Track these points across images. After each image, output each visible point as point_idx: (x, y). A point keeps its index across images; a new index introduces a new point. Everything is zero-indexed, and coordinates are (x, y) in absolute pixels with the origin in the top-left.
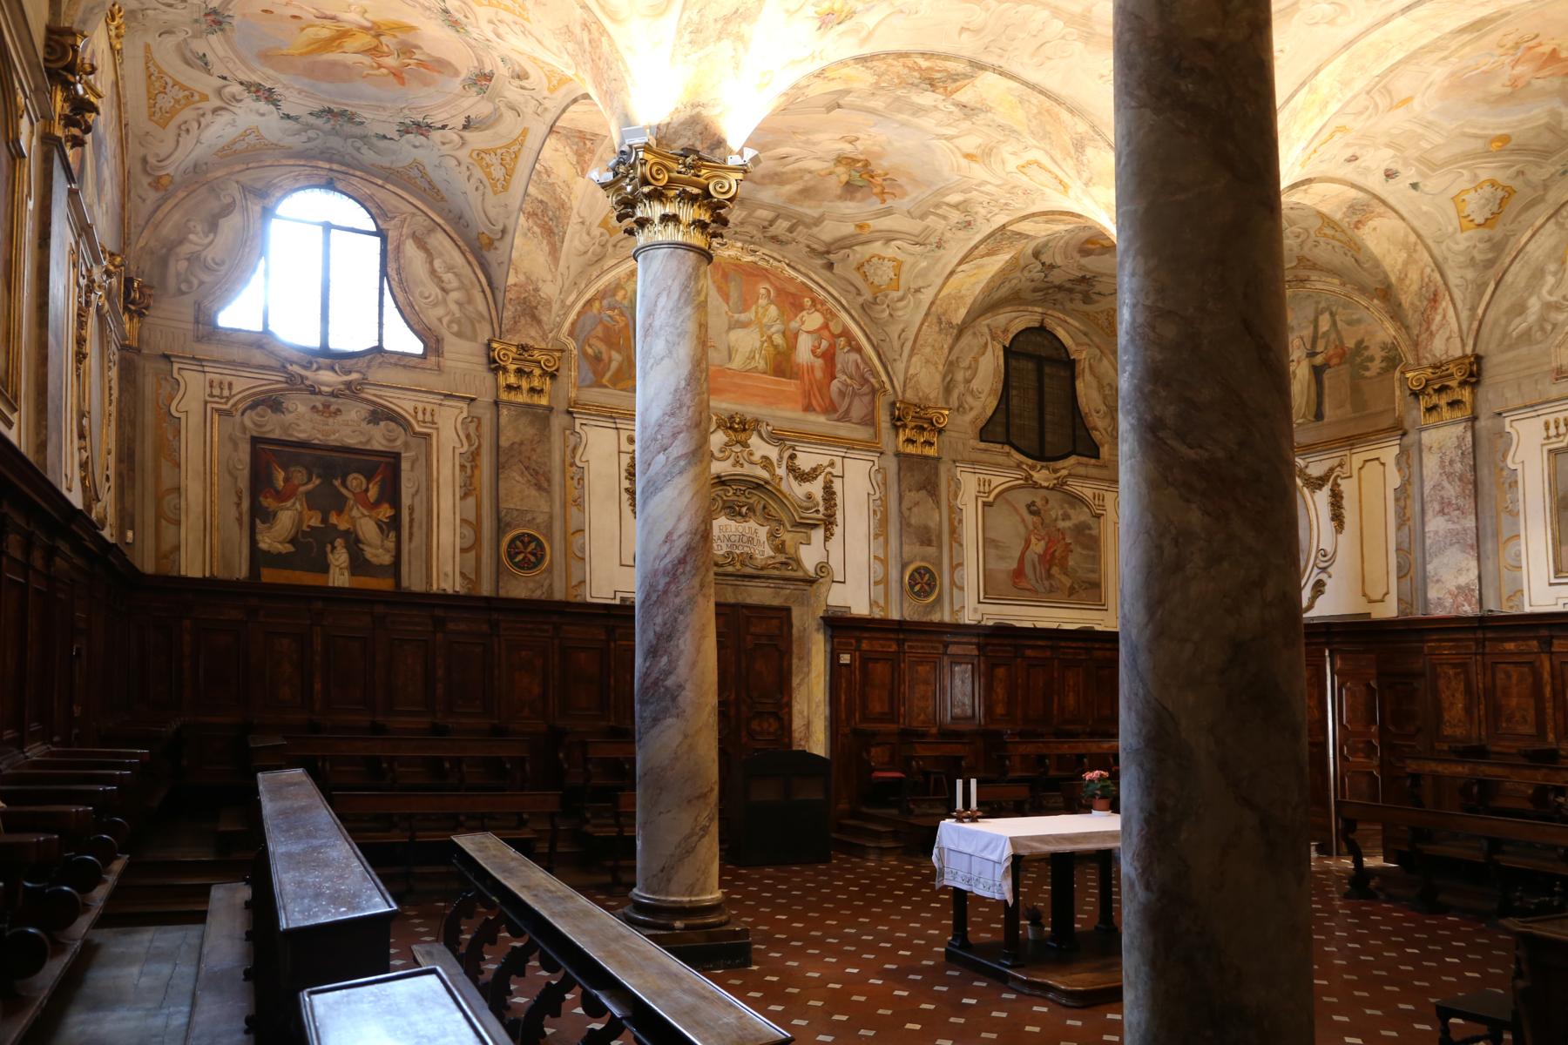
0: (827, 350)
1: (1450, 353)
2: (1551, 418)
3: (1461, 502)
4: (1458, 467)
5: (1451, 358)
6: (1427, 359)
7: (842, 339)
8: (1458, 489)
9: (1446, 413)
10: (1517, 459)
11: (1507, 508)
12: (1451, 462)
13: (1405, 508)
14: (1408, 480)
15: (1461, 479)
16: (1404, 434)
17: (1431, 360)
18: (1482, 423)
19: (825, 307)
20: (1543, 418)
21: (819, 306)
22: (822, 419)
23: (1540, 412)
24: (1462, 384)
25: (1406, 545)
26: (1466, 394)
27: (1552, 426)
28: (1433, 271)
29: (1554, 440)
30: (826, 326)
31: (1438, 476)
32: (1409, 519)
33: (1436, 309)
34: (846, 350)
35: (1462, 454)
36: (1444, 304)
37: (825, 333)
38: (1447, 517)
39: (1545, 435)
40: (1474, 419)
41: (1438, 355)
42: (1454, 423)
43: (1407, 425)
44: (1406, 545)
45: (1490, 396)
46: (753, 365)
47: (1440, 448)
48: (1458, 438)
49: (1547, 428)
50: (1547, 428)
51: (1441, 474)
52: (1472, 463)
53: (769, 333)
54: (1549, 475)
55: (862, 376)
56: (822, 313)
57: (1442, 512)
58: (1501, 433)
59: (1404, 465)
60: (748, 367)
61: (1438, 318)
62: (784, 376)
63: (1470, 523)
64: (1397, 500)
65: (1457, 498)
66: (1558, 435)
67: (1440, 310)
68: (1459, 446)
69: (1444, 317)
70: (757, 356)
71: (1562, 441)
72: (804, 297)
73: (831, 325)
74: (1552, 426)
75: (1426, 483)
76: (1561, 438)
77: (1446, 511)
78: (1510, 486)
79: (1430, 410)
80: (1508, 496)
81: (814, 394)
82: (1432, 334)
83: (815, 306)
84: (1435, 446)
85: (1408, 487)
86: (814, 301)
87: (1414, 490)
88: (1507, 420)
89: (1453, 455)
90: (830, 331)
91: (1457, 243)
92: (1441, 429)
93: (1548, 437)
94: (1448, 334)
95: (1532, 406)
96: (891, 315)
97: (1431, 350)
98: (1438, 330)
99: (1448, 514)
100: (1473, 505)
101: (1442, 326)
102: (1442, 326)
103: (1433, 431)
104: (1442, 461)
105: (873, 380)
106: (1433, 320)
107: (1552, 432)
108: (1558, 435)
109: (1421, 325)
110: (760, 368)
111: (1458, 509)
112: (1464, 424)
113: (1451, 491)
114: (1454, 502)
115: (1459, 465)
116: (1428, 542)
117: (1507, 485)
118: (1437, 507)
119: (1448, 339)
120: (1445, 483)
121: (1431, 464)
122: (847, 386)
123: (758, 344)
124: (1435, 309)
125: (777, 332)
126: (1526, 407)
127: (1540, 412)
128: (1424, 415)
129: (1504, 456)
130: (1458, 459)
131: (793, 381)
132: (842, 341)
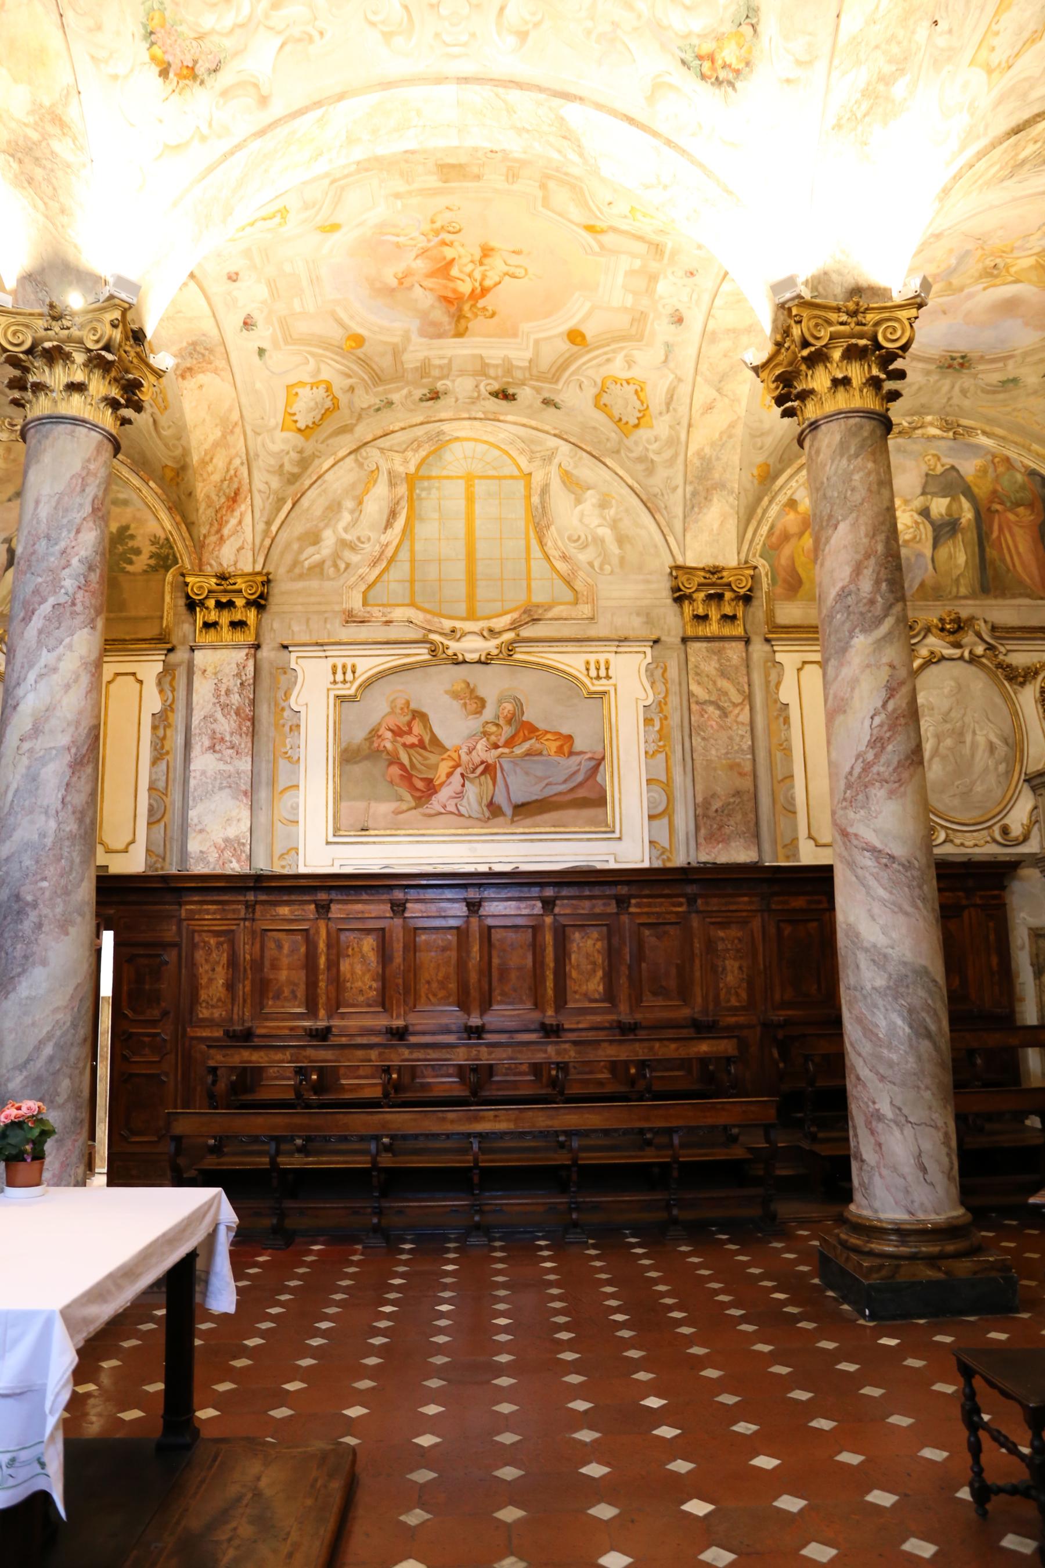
1: (240, 565)
2: (339, 662)
3: (236, 739)
4: (235, 699)
5: (239, 572)
6: (211, 565)
8: (234, 725)
9: (226, 634)
10: (301, 701)
11: (286, 753)
12: (228, 692)
13: (164, 738)
14: (170, 706)
15: (237, 713)
16: (171, 650)
17: (217, 569)
18: (264, 653)
20: (331, 661)
23: (328, 654)
24: (249, 604)
25: (161, 785)
26: (251, 616)
27: (340, 671)
28: (242, 464)
29: (340, 686)
31: (211, 705)
32: (168, 753)
33: (233, 511)
35: (242, 684)
36: (243, 507)
38: (218, 756)
39: (332, 679)
40: (257, 647)
41: (225, 565)
42: (237, 647)
43: (175, 640)
44: (161, 785)
45: (276, 625)
47: (215, 674)
48: (238, 665)
49: (334, 673)
50: (334, 673)
51: (214, 704)
52: (251, 696)
54: (335, 723)
57: (212, 748)
58: (285, 669)
59: (167, 687)
61: (233, 522)
63: (244, 765)
64: (155, 728)
65: (232, 734)
66: (345, 682)
67: (237, 514)
68: (238, 675)
69: (240, 522)
71: (349, 689)
74: (340, 671)
75: (195, 712)
76: (348, 685)
77: (217, 748)
78: (291, 730)
79: (207, 625)
80: (288, 740)
82: (222, 539)
84: (210, 670)
85: (169, 713)
87: (178, 718)
88: (293, 655)
89: (231, 683)
91: (273, 442)
92: (219, 652)
93: (335, 682)
94: (239, 544)
95: (322, 645)
97: (217, 557)
98: (230, 536)
99: (220, 751)
100: (250, 745)
101: (235, 532)
102: (235, 532)
103: (209, 652)
104: (217, 689)
106: (227, 522)
107: (339, 677)
108: (345, 682)
109: (211, 525)
111: (233, 748)
112: (246, 651)
113: (225, 725)
114: (228, 738)
115: (237, 696)
116: (192, 783)
117: (287, 728)
118: (207, 743)
119: (242, 548)
120: (219, 715)
121: (203, 690)
124: (231, 509)
126: (317, 644)
127: (328, 654)
128: (201, 632)
129: (287, 695)
130: (236, 689)
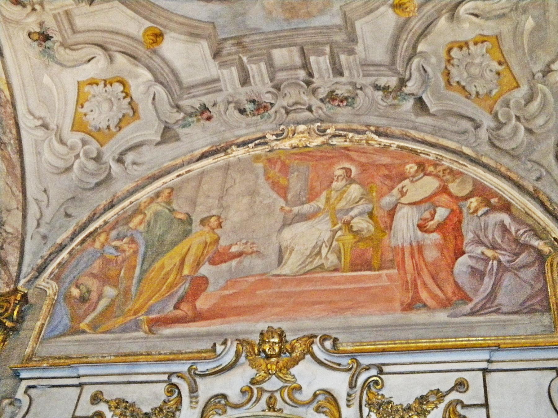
0: (447, 218)
7: (473, 200)
19: (440, 168)
21: (431, 169)
22: (442, 316)
30: (444, 190)
34: (480, 213)
37: (444, 198)
46: (317, 262)
53: (346, 218)
55: (516, 241)
56: (437, 176)
60: (308, 268)
62: (370, 270)
70: (324, 251)
72: (405, 164)
73: (454, 188)
81: (425, 284)
83: (422, 170)
86: (421, 166)
90: (450, 194)
96: (529, 131)
105: (537, 243)
110: (327, 265)
122: (487, 260)
123: (327, 236)
125: (360, 214)
131: (384, 272)
132: (474, 202)
